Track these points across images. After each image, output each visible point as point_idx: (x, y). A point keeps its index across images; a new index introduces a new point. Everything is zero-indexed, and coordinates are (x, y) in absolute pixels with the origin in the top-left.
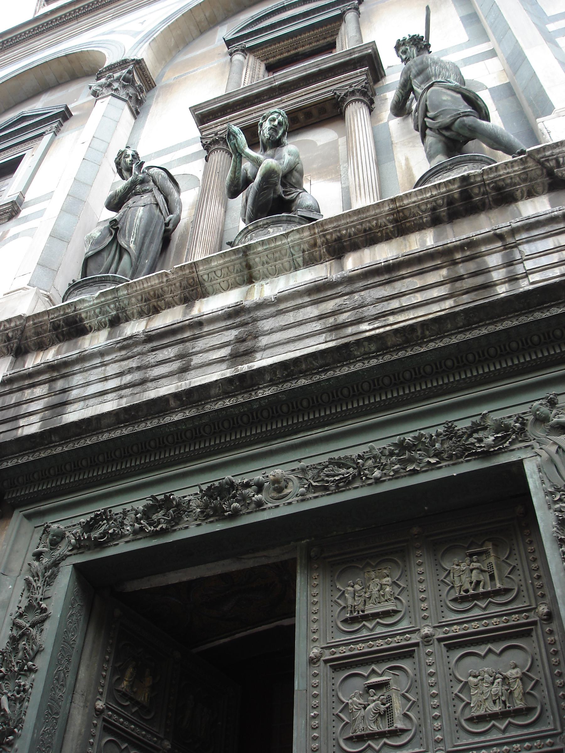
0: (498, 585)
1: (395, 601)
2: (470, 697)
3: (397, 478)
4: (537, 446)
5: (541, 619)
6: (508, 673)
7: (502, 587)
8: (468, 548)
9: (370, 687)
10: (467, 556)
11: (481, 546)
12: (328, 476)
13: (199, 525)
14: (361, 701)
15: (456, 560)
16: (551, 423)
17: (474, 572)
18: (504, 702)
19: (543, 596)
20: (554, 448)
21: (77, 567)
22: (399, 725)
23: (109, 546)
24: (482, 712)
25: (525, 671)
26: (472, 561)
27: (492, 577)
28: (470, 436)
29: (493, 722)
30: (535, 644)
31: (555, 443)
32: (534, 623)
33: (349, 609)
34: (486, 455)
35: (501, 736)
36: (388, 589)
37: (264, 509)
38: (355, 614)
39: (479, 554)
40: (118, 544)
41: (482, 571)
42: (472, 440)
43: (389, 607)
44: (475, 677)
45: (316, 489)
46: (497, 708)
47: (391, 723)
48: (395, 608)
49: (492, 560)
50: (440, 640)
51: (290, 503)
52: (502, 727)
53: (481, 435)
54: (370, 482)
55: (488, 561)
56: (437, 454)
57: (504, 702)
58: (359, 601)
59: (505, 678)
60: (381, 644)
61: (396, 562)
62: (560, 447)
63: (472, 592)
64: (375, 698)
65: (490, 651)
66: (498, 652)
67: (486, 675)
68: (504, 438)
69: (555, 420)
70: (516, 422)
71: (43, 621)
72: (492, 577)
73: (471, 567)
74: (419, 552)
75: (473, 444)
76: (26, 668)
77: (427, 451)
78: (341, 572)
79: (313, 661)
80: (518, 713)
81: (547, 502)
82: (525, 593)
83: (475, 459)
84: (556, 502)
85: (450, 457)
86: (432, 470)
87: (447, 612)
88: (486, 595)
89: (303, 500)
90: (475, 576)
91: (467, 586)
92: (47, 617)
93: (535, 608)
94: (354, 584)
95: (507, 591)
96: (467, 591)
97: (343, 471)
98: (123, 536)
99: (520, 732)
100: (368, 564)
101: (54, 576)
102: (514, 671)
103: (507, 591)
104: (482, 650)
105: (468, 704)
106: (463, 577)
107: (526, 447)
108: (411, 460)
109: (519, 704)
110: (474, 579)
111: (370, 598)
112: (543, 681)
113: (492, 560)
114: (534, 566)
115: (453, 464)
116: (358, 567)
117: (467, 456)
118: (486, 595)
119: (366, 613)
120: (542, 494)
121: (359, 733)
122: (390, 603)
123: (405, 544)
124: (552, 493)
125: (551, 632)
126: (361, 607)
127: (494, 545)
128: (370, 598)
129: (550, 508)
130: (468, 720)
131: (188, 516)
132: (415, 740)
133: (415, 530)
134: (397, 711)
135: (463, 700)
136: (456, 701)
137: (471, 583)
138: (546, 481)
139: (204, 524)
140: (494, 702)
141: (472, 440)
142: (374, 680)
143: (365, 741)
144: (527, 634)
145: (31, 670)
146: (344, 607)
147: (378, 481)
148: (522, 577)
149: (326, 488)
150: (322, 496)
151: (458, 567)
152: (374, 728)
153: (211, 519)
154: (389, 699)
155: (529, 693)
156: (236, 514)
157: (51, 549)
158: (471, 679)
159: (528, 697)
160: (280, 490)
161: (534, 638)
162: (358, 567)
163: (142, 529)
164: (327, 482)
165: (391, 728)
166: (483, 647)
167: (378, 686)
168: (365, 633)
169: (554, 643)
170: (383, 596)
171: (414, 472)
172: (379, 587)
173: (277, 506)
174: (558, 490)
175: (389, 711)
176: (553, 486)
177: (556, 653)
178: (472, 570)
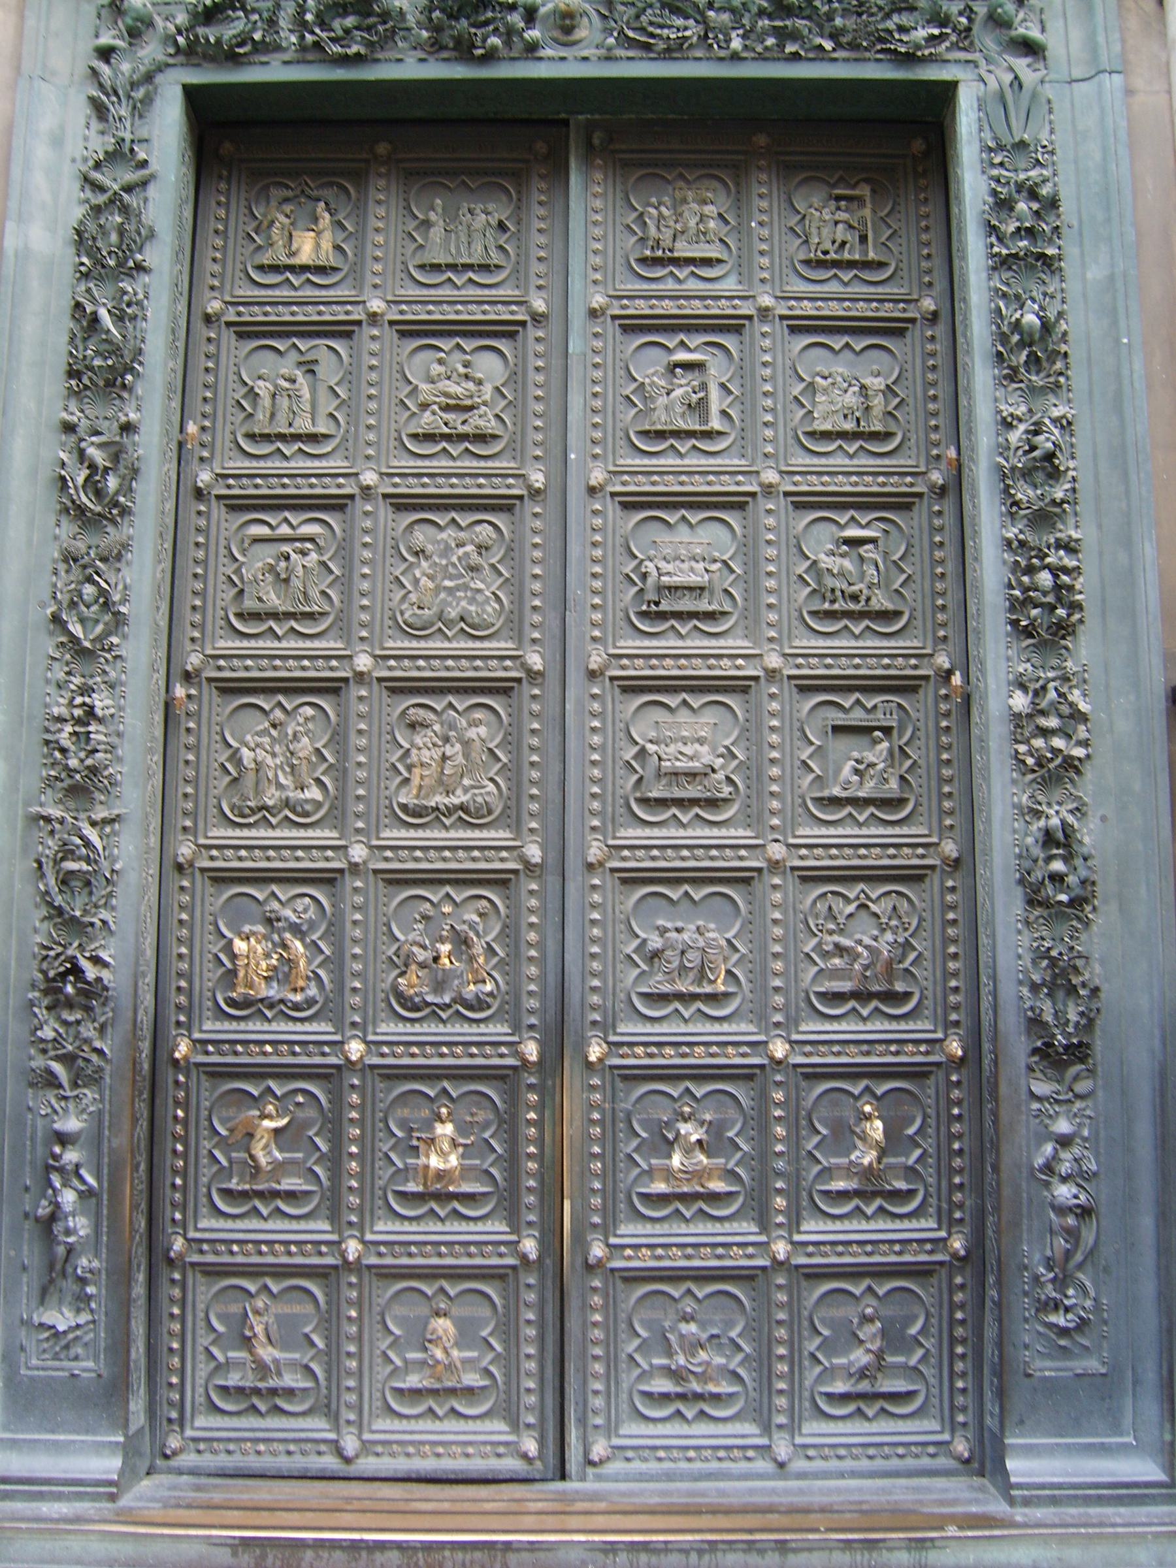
0: (872, 255)
1: (718, 243)
2: (814, 403)
3: (766, 59)
4: (982, 63)
5: (923, 318)
6: (868, 381)
7: (876, 258)
8: (834, 186)
9: (677, 365)
10: (830, 197)
11: (854, 187)
12: (651, 23)
13: (422, 60)
14: (663, 383)
15: (816, 201)
16: (1013, 33)
17: (840, 226)
18: (858, 420)
19: (930, 284)
20: (1008, 78)
21: (192, 94)
22: (716, 424)
23: (250, 63)
24: (827, 426)
25: (889, 382)
26: (838, 208)
27: (863, 239)
28: (888, 16)
29: (839, 442)
30: (908, 349)
31: (1011, 69)
32: (912, 321)
33: (651, 243)
34: (910, 59)
35: (847, 461)
36: (712, 224)
37: (540, 59)
38: (660, 253)
39: (849, 199)
40: (267, 63)
41: (851, 227)
42: (890, 24)
43: (712, 252)
44: (825, 378)
45: (632, 43)
46: (849, 426)
47: (705, 419)
48: (719, 256)
49: (867, 212)
50: (782, 318)
51: (585, 59)
52: (851, 451)
53: (904, 19)
54: (722, 54)
55: (860, 213)
56: (834, 36)
57: (858, 420)
58: (667, 235)
59: (863, 387)
60: (697, 308)
61: (725, 184)
62: (1016, 77)
63: (833, 256)
64: (683, 381)
65: (847, 345)
66: (858, 349)
67: (839, 379)
68: (942, 37)
69: (1021, 31)
70: (961, 14)
71: (144, 184)
72: (863, 239)
73: (837, 217)
74: (764, 177)
75: (890, 32)
76: (131, 264)
77: (821, 27)
78: (639, 179)
79: (593, 313)
80: (874, 436)
81: (982, 161)
82: (905, 274)
83: (890, 60)
84: (993, 165)
85: (854, 46)
86: (822, 59)
87: (794, 279)
88: (851, 264)
89: (608, 59)
90: (841, 233)
91: (827, 245)
92: (152, 177)
93: (917, 301)
94: (660, 204)
95: (881, 265)
96: (825, 253)
97: (680, 22)
98: (278, 48)
99: (871, 462)
100: (682, 176)
101: (148, 100)
102: (876, 381)
103: (881, 265)
104: (837, 342)
105: (811, 412)
106: (825, 232)
107: (967, 62)
108: (795, 36)
109: (878, 427)
110: (839, 237)
111: (683, 233)
112: (911, 401)
113: (867, 212)
114: (924, 237)
115: (856, 60)
116: (663, 177)
117: (879, 52)
118: (851, 264)
119: (676, 254)
120: (976, 146)
121: (659, 427)
122: (712, 247)
123: (741, 157)
124: (991, 150)
125: (933, 338)
126: (667, 243)
127: (873, 191)
128: (683, 233)
129: (983, 172)
130: (806, 433)
131: (405, 39)
132: (734, 448)
133: (762, 140)
134: (714, 407)
135: (803, 406)
136: (794, 406)
137: (834, 242)
138: (986, 127)
139: (431, 59)
140: (845, 416)
141: (890, 24)
142: (682, 356)
143: (665, 439)
144: (899, 333)
145: (140, 268)
146: (642, 239)
147: (735, 57)
148: (904, 249)
149: (647, 47)
150: (641, 59)
151: (817, 214)
152: (682, 425)
153: (445, 55)
154: (704, 386)
155: (890, 413)
156: (490, 57)
157: (131, 44)
158: (818, 379)
159: (890, 419)
160: (568, 30)
161: (908, 340)
162: (663, 177)
163: (317, 45)
164: (652, 36)
165: (704, 428)
166: (837, 337)
167: (688, 366)
168: (670, 284)
169: (933, 355)
170: (704, 234)
171: (795, 57)
172: (698, 218)
173: (563, 59)
174: (1001, 148)
175: (703, 404)
176: (996, 138)
177: (934, 367)
178: (836, 223)
